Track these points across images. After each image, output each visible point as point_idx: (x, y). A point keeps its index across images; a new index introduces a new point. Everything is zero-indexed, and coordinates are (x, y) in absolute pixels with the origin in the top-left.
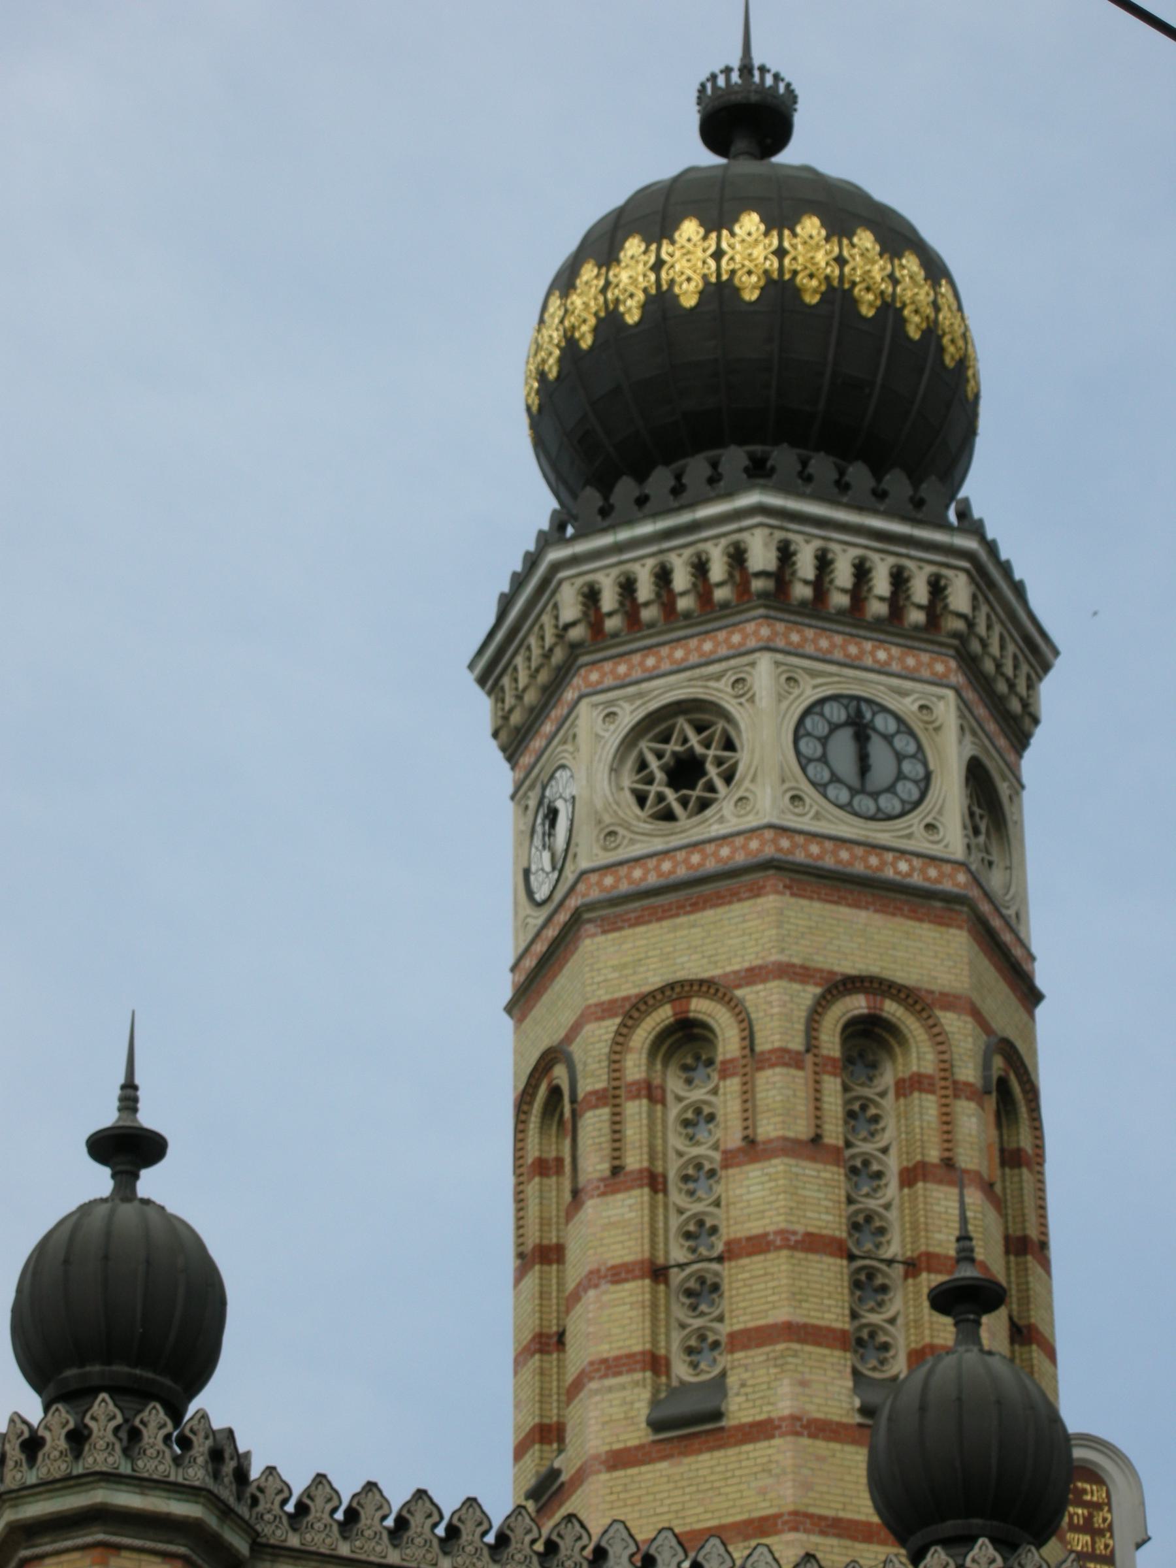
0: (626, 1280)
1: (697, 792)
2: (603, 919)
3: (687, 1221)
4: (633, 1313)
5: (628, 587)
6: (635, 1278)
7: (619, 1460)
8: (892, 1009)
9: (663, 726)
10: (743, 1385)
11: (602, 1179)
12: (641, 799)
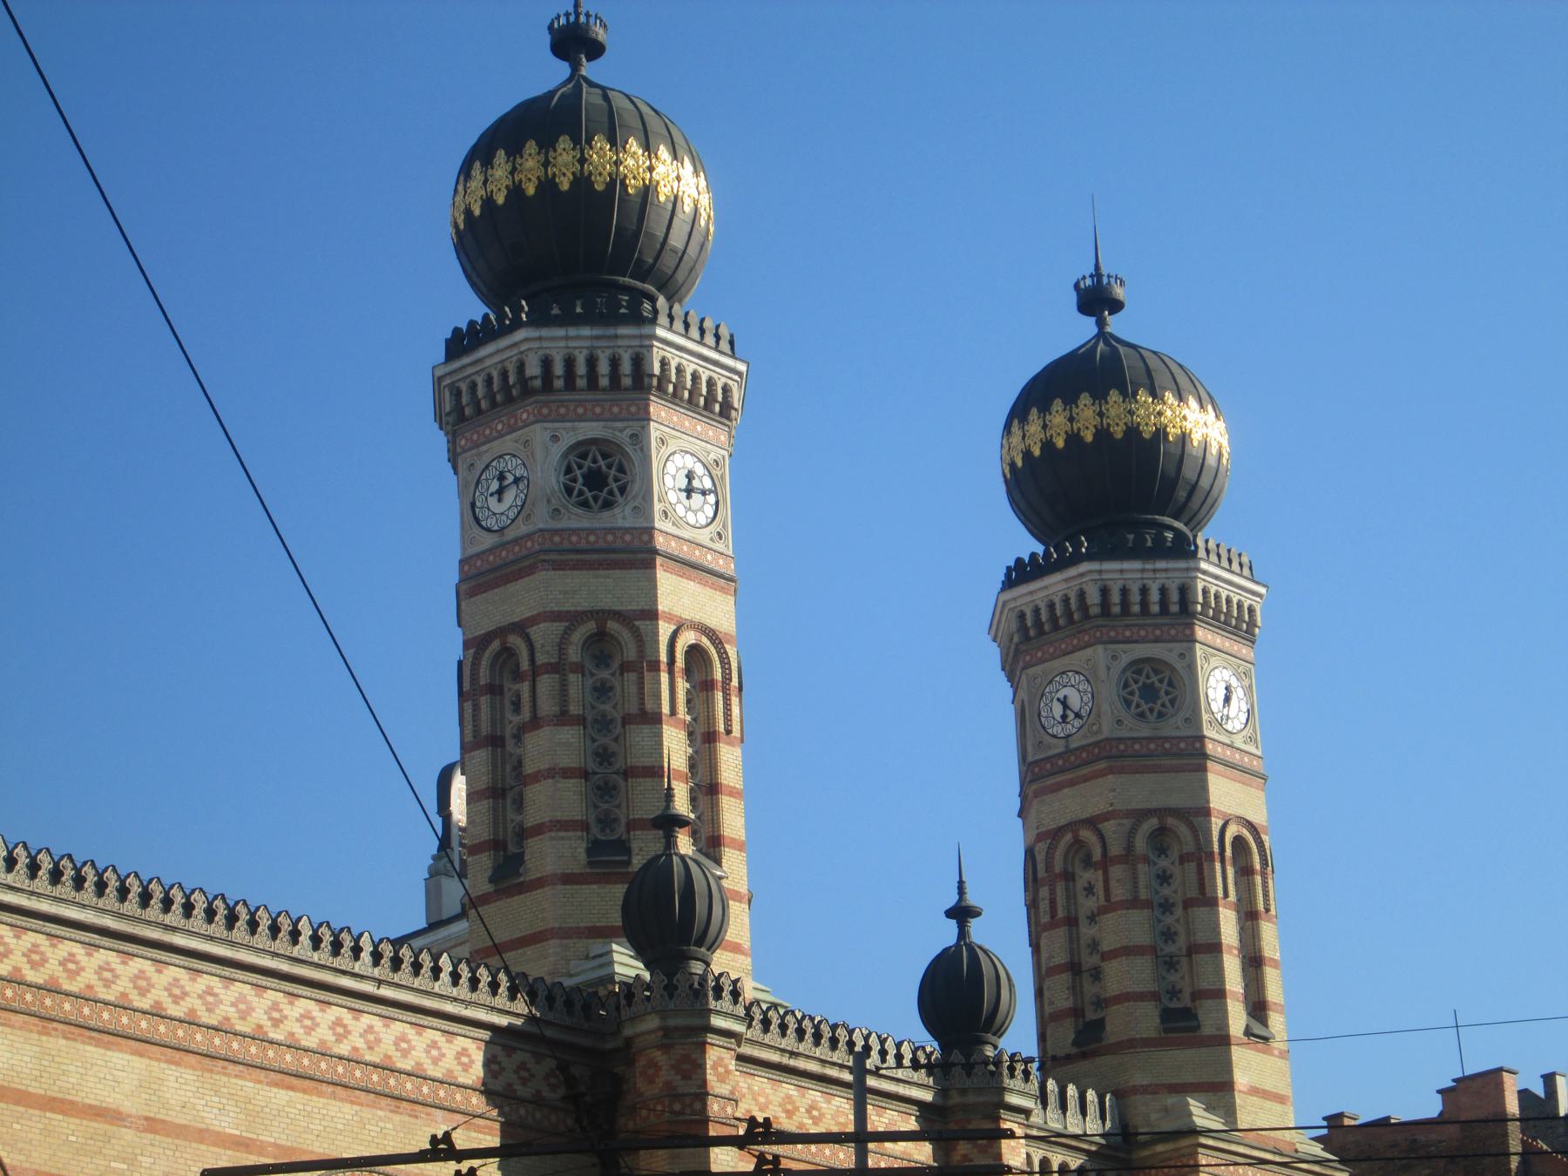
0: (571, 778)
1: (604, 494)
2: (553, 561)
3: (598, 747)
4: (575, 797)
5: (569, 363)
6: (576, 777)
7: (568, 879)
8: (705, 642)
9: (582, 449)
10: (641, 850)
11: (554, 716)
12: (569, 491)
